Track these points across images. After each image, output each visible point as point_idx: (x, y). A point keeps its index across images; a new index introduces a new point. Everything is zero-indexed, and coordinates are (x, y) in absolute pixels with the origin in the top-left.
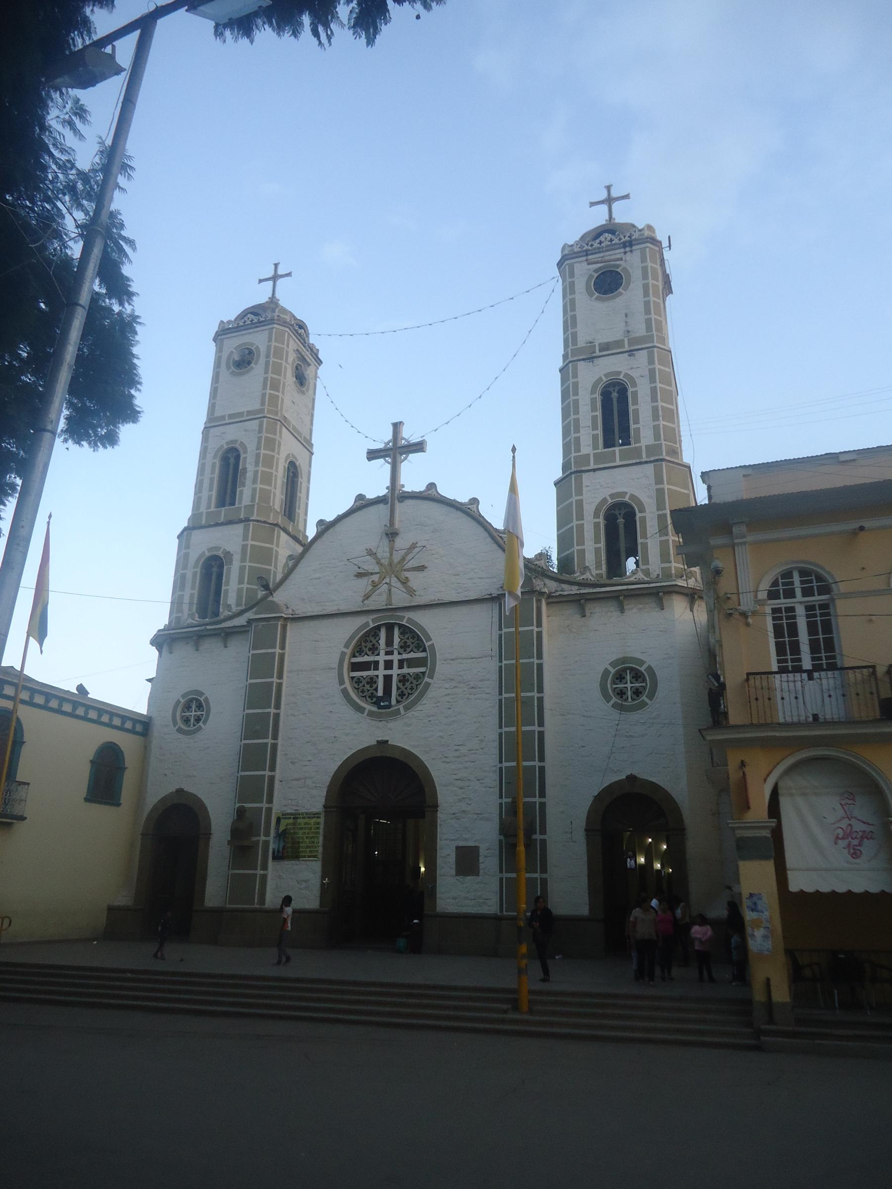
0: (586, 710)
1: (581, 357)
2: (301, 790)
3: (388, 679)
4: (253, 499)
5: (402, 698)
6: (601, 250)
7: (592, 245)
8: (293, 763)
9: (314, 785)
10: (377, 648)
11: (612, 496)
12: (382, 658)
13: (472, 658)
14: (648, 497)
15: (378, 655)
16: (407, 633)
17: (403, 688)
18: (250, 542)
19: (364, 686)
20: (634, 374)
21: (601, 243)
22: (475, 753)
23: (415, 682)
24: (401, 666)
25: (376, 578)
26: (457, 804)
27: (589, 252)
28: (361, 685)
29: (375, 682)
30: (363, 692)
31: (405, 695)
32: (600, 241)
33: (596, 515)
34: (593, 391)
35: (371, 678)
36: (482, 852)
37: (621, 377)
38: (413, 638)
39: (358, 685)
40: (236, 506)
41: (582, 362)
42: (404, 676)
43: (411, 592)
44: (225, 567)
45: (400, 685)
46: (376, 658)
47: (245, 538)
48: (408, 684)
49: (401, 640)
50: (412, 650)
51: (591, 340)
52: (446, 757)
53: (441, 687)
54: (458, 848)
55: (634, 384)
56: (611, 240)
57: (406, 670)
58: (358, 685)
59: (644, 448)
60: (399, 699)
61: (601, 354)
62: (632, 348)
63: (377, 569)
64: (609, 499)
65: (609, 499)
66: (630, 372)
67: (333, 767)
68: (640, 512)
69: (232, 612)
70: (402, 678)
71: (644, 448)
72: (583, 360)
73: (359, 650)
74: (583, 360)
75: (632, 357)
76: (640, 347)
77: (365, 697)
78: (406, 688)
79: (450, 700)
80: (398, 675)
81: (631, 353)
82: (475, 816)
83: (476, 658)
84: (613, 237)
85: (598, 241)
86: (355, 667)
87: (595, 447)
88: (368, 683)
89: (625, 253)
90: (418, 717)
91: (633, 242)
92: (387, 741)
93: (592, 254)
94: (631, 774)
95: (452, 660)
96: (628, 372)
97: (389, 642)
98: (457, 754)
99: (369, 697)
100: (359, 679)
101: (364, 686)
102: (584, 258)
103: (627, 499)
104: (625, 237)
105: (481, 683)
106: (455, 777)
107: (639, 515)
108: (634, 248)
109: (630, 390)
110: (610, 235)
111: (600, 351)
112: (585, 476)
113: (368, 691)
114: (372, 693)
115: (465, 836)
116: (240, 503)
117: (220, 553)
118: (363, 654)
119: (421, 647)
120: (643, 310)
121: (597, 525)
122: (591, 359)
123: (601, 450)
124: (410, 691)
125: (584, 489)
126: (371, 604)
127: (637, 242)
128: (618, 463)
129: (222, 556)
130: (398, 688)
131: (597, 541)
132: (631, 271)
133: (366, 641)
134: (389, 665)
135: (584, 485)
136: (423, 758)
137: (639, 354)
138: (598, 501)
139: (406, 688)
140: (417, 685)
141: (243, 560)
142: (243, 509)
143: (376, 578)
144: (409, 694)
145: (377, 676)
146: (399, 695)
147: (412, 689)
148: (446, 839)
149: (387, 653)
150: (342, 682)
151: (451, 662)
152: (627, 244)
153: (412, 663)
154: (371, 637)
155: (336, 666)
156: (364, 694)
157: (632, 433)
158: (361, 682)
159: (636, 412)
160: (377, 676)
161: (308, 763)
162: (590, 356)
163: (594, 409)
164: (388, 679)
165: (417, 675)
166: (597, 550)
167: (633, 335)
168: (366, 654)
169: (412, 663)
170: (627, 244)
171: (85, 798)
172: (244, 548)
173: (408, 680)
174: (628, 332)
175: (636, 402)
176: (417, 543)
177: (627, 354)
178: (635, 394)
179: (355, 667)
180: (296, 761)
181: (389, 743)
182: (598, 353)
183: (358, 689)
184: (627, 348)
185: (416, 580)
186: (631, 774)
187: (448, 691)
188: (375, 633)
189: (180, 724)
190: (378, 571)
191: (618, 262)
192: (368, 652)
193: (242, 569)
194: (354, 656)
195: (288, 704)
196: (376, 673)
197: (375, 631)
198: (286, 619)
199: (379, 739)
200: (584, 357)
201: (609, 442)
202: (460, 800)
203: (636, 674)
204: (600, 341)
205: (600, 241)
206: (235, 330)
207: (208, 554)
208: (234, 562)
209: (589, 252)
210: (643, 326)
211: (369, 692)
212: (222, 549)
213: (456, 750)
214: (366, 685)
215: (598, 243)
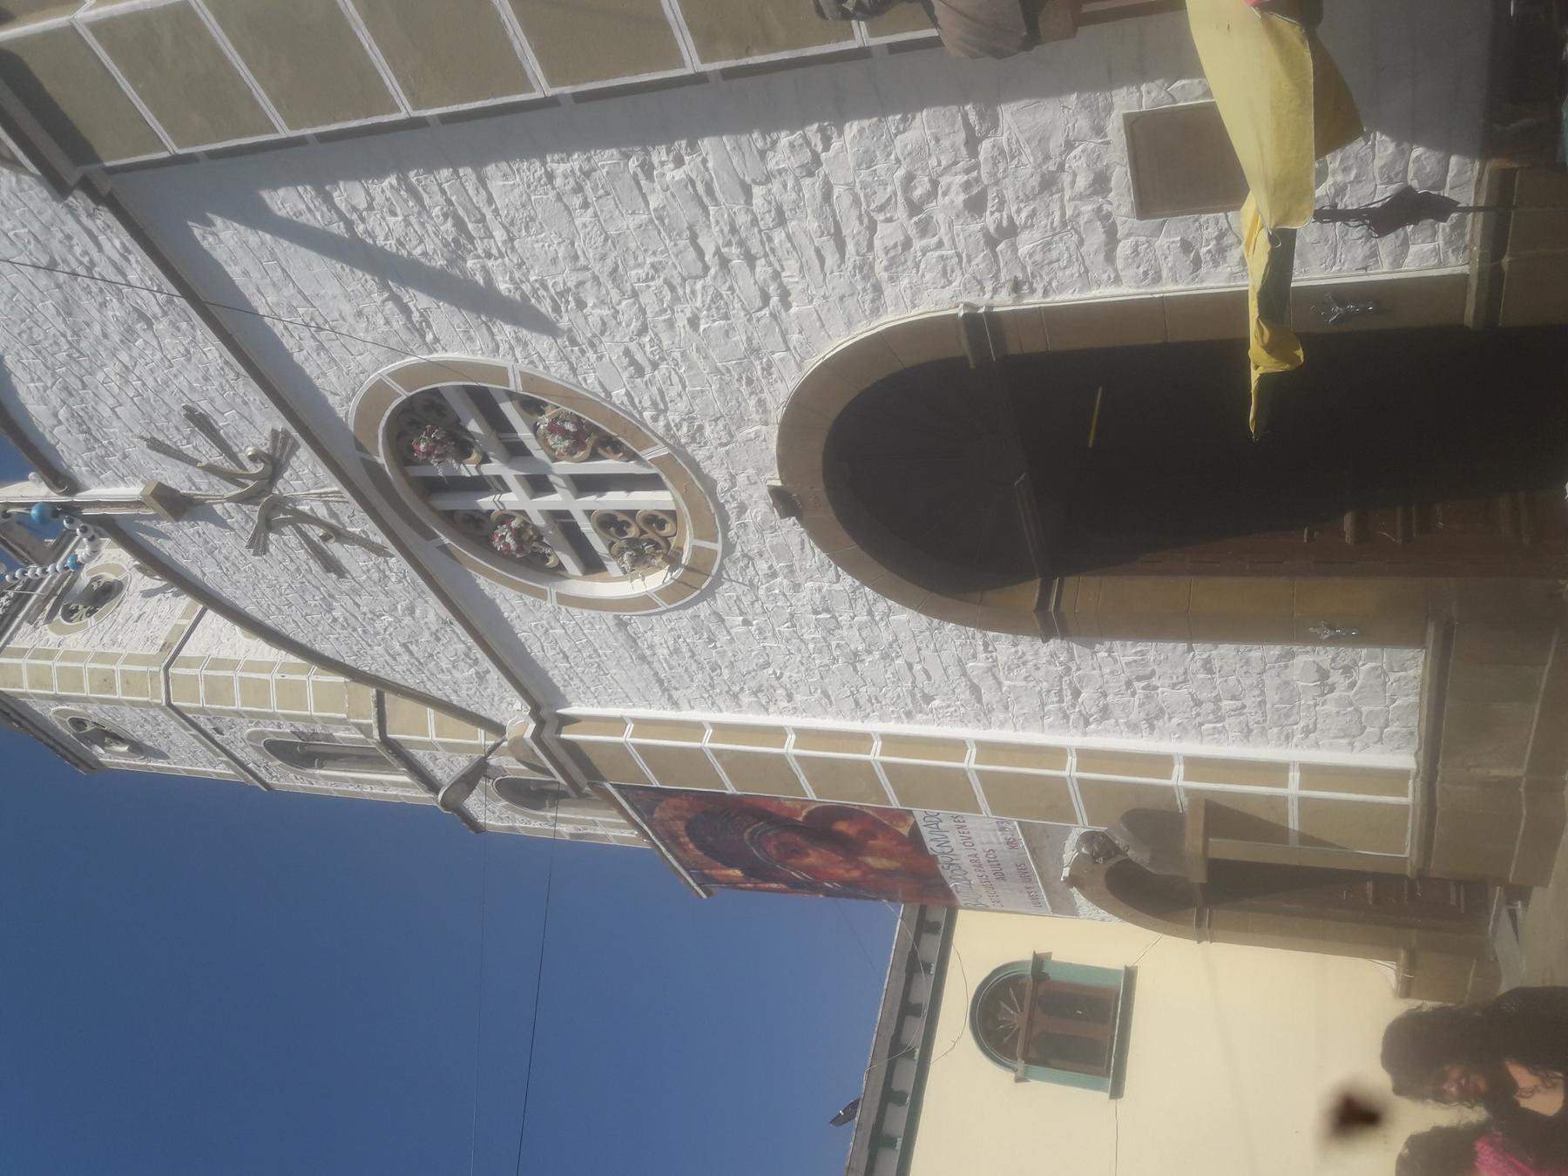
106: (831, 260)
202: (925, 228)
206: (57, 747)
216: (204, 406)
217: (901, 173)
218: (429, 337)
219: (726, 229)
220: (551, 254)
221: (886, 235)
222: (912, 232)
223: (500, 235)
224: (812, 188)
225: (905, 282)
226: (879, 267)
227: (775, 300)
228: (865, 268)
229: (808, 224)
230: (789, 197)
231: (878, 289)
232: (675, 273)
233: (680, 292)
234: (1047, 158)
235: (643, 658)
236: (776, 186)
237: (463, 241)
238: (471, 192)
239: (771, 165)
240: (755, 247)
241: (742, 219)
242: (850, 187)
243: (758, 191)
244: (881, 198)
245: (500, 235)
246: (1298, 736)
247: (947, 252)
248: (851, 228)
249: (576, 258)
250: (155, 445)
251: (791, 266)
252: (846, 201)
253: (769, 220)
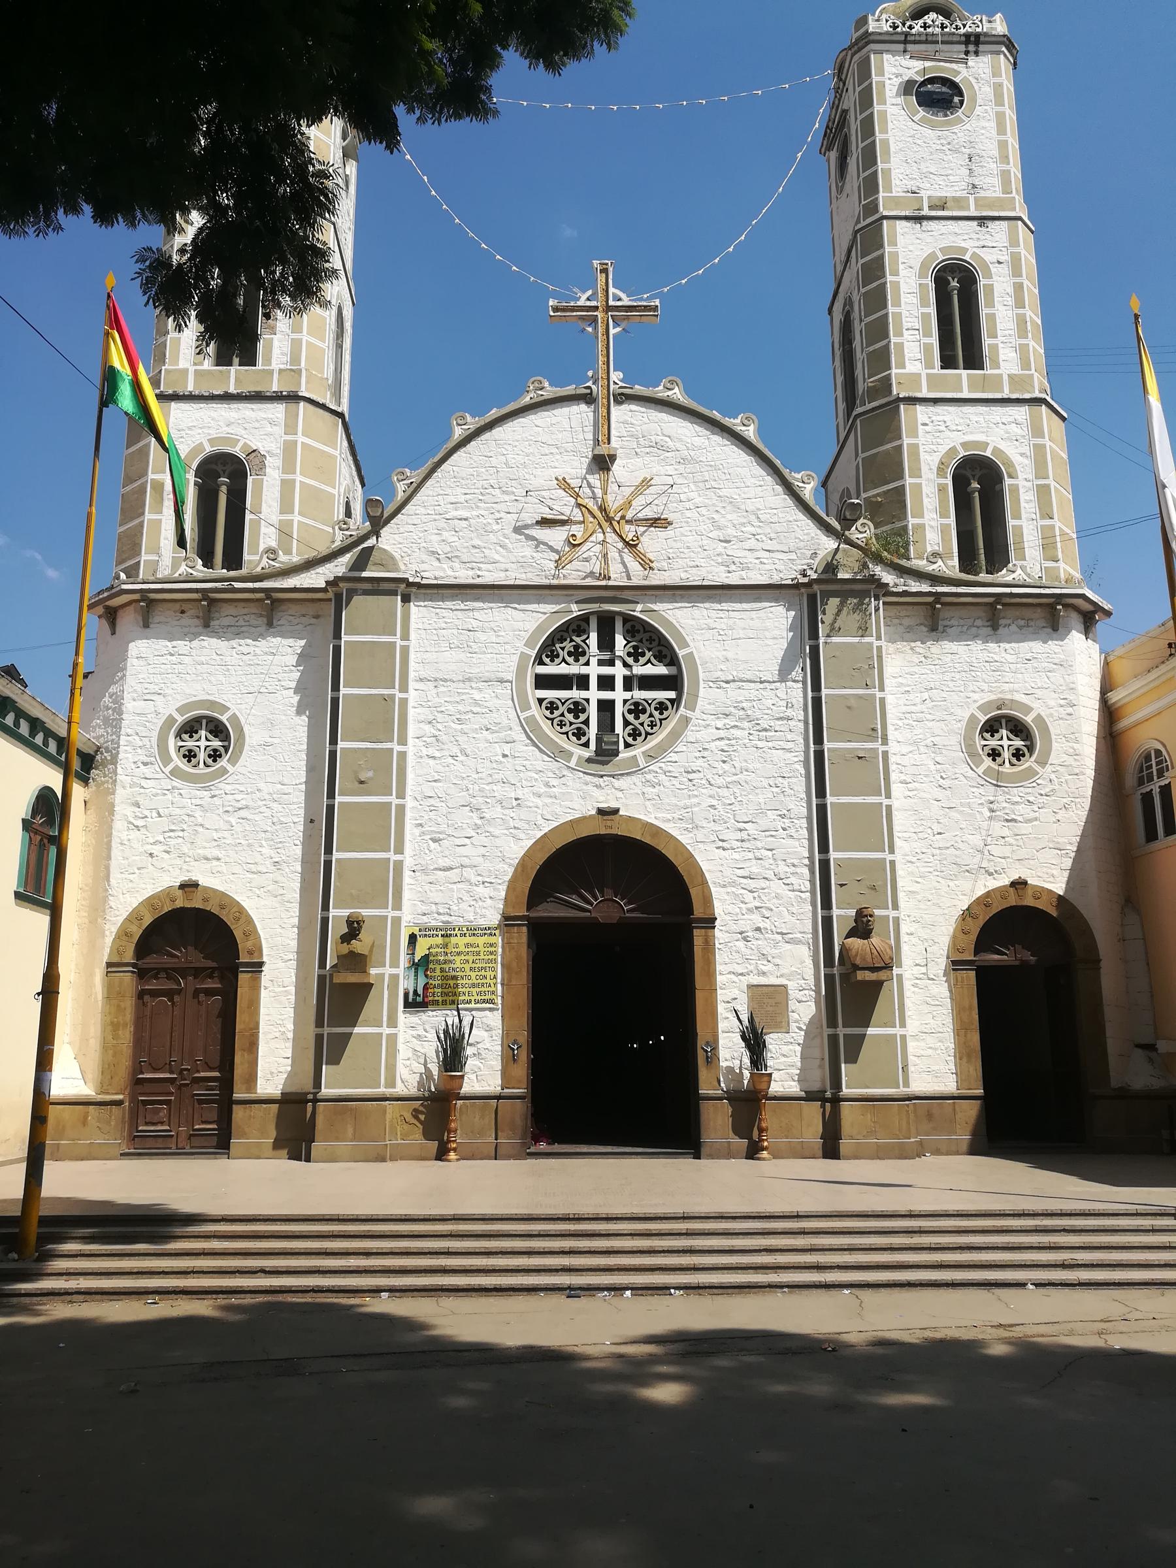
0: (942, 777)
1: (903, 214)
2: (454, 886)
3: (606, 707)
4: (295, 359)
5: (635, 739)
6: (930, 38)
7: (911, 27)
8: (434, 840)
9: (480, 879)
10: (584, 654)
11: (964, 445)
12: (594, 671)
13: (761, 682)
14: (1022, 455)
15: (587, 664)
16: (638, 631)
17: (636, 723)
18: (301, 439)
19: (562, 715)
20: (989, 256)
21: (925, 26)
22: (772, 836)
23: (656, 713)
24: (628, 686)
25: (577, 530)
26: (746, 917)
27: (909, 38)
28: (557, 713)
29: (584, 711)
30: (561, 724)
31: (640, 735)
32: (925, 24)
33: (941, 471)
34: (922, 275)
35: (576, 704)
36: (793, 993)
37: (967, 258)
38: (651, 640)
39: (552, 713)
40: (260, 366)
41: (904, 223)
42: (636, 704)
43: (646, 564)
44: (250, 480)
45: (630, 718)
46: (584, 670)
47: (290, 428)
48: (643, 717)
49: (629, 642)
50: (649, 661)
51: (914, 188)
52: (723, 841)
53: (708, 725)
54: (751, 987)
55: (989, 276)
56: (943, 27)
57: (639, 695)
58: (552, 713)
59: (1005, 378)
60: (630, 740)
61: (933, 213)
62: (985, 214)
63: (577, 515)
64: (959, 448)
65: (959, 448)
66: (980, 252)
67: (517, 849)
68: (1010, 476)
69: (281, 562)
70: (633, 707)
71: (1005, 378)
72: (906, 218)
73: (548, 651)
74: (906, 218)
75: (983, 229)
76: (996, 214)
77: (567, 733)
78: (642, 724)
79: (726, 748)
80: (625, 701)
81: (982, 220)
82: (779, 937)
83: (769, 682)
84: (946, 22)
85: (921, 22)
86: (542, 682)
87: (929, 365)
88: (570, 710)
89: (967, 53)
90: (670, 772)
91: (982, 38)
92: (616, 811)
93: (915, 42)
94: (1020, 877)
95: (727, 682)
96: (977, 251)
97: (606, 643)
98: (744, 835)
99: (574, 734)
100: (552, 703)
101: (562, 715)
102: (901, 47)
103: (988, 453)
104: (964, 26)
105: (781, 722)
106: (740, 872)
107: (1008, 481)
108: (982, 48)
109: (982, 282)
110: (941, 18)
111: (931, 208)
112: (919, 408)
113: (571, 724)
114: (579, 729)
115: (764, 969)
116: (268, 361)
117: (237, 450)
118: (557, 661)
119: (666, 654)
120: (996, 153)
121: (942, 489)
122: (918, 219)
123: (937, 370)
124: (649, 729)
125: (921, 427)
126: (573, 574)
127: (987, 39)
128: (965, 394)
129: (242, 456)
130: (626, 723)
131: (944, 514)
132: (976, 87)
133: (562, 640)
134: (606, 683)
135: (920, 422)
136: (684, 839)
137: (993, 225)
138: (943, 449)
139: (642, 724)
140: (661, 720)
141: (288, 465)
142: (276, 376)
143: (577, 530)
144: (647, 734)
145: (587, 700)
146: (629, 735)
147: (652, 725)
148: (730, 973)
149: (601, 663)
150: (526, 707)
151: (725, 685)
152: (972, 39)
153: (648, 683)
154: (570, 630)
155: (511, 676)
156: (565, 729)
157: (986, 350)
158: (557, 708)
159: (992, 318)
160: (587, 700)
161: (467, 841)
162: (916, 213)
163: (924, 303)
164: (606, 707)
165: (661, 703)
166: (944, 529)
167: (982, 194)
168: (564, 660)
169: (648, 683)
170: (972, 39)
171: (18, 895)
172: (289, 450)
173: (644, 711)
174: (974, 186)
175: (991, 304)
176: (650, 480)
177: (975, 223)
178: (990, 289)
179: (542, 682)
180: (441, 836)
181: (621, 813)
182: (926, 212)
183: (552, 720)
184: (973, 212)
185: (652, 542)
186: (1020, 877)
187: (722, 734)
188: (579, 626)
189: (178, 762)
190: (582, 519)
191: (954, 66)
192: (567, 658)
193: (287, 487)
194: (541, 663)
195: (418, 738)
196: (584, 694)
197: (577, 627)
198: (410, 584)
199: (603, 805)
200: (908, 213)
201: (948, 362)
203: (1016, 726)
204: (929, 193)
205: (925, 24)
207: (209, 449)
208: (268, 470)
209: (902, 38)
210: (996, 181)
211: (574, 726)
212: (240, 444)
213: (741, 830)
214: (566, 713)
215: (921, 27)
216: (669, 532)
217: (773, 908)
218: (711, 684)
219: (755, 837)
220: (749, 762)
221: (749, 897)
222: (749, 906)
223: (760, 744)
224: (770, 874)
225: (726, 897)
226: (734, 889)
227: (721, 844)
228: (733, 884)
229: (755, 869)
230: (766, 863)
231: (724, 886)
232: (737, 809)
233: (728, 807)
234: (773, 958)
235: (469, 680)
236: (772, 861)
237: (758, 727)
238: (780, 743)
239: (779, 862)
240: (745, 845)
241: (759, 844)
242: (769, 887)
243: (769, 853)
244: (763, 898)
245: (760, 744)
246: (415, 1033)
247: (740, 916)
248: (752, 884)
249: (747, 771)
250: (646, 483)
251: (736, 856)
252: (764, 885)
253: (758, 855)
